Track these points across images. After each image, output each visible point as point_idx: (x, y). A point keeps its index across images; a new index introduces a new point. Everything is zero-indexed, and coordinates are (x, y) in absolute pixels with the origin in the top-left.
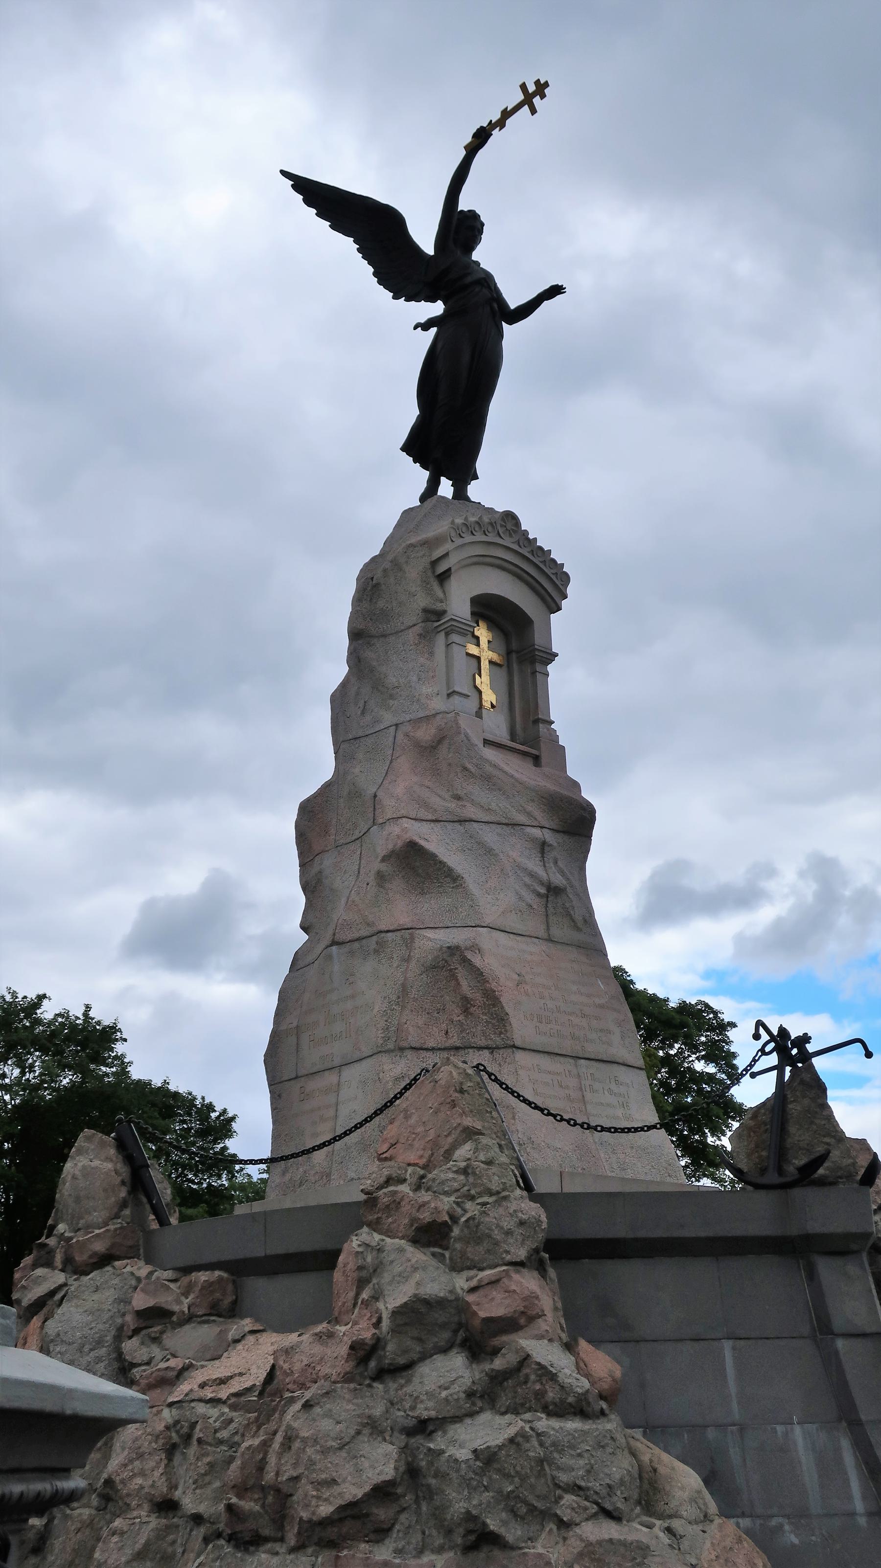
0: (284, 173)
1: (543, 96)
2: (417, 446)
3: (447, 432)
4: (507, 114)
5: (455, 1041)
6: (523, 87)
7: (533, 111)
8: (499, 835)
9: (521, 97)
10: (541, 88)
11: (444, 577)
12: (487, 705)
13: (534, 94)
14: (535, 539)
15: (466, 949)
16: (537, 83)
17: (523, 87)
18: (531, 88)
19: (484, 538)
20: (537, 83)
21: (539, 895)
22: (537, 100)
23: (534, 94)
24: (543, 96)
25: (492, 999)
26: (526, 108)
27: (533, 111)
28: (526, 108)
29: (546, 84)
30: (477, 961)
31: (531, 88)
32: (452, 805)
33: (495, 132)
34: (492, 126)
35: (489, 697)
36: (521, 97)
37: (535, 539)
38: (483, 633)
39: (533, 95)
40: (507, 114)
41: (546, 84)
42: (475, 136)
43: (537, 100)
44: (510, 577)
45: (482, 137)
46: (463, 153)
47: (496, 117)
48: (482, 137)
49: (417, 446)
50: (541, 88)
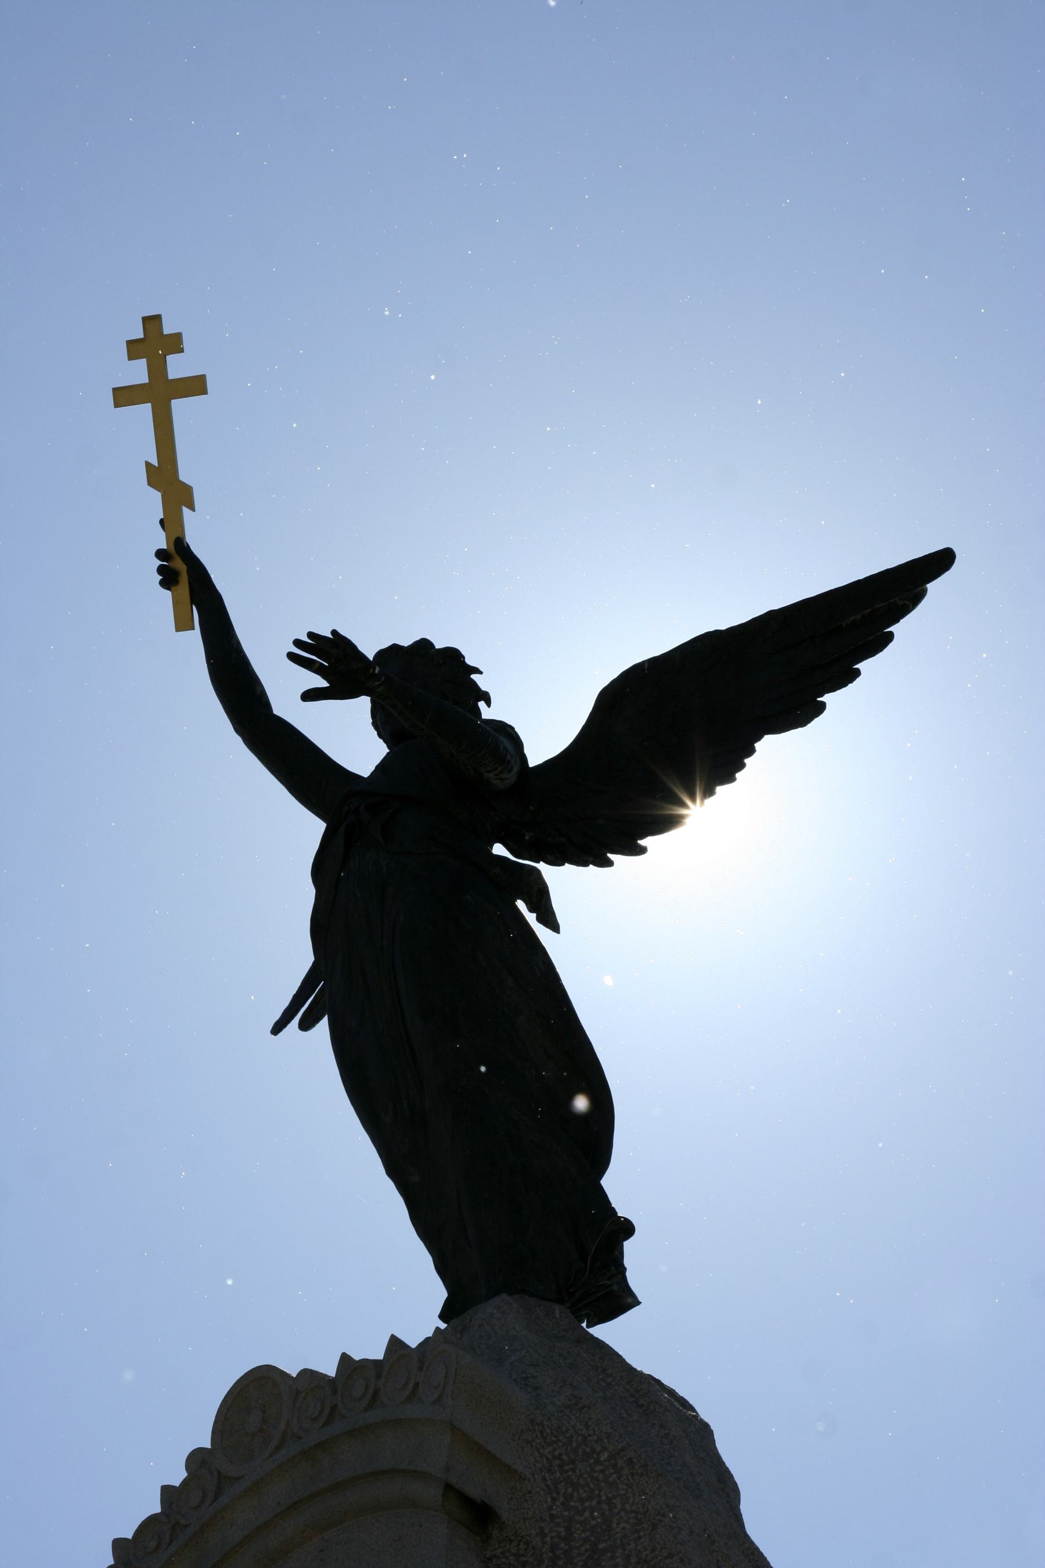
1: (175, 343)
6: (124, 396)
7: (196, 386)
9: (144, 412)
10: (154, 342)
13: (157, 369)
14: (395, 1343)
16: (134, 349)
17: (124, 396)
18: (138, 373)
20: (134, 349)
22: (177, 367)
23: (157, 369)
24: (175, 343)
26: (180, 407)
27: (196, 386)
28: (180, 407)
29: (152, 322)
31: (138, 373)
34: (171, 522)
36: (144, 412)
37: (395, 1343)
39: (159, 375)
41: (152, 322)
42: (168, 579)
43: (177, 367)
46: (194, 638)
47: (153, 502)
50: (154, 342)
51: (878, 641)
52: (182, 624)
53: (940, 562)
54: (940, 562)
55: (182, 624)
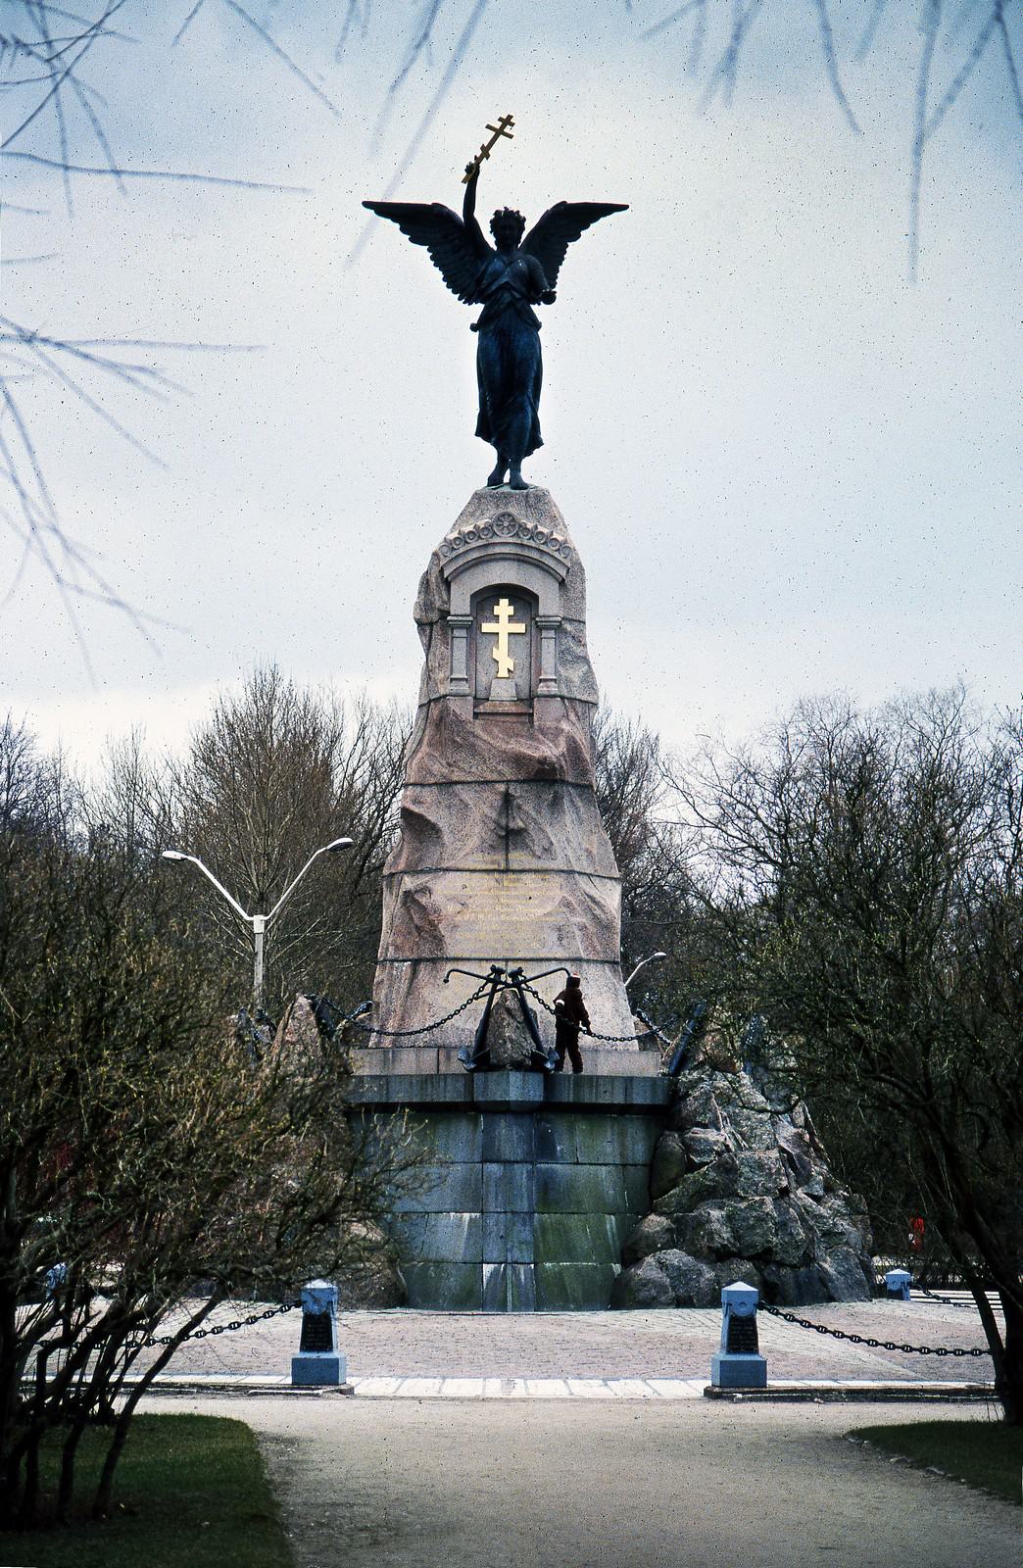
0: (367, 204)
1: (512, 125)
2: (484, 431)
3: (509, 407)
4: (485, 151)
5: (414, 956)
7: (511, 137)
8: (476, 791)
10: (507, 121)
11: (447, 584)
12: (503, 673)
13: (503, 127)
15: (416, 892)
16: (500, 119)
18: (498, 125)
19: (480, 543)
20: (500, 119)
21: (500, 837)
22: (507, 130)
25: (434, 926)
27: (511, 137)
28: (501, 137)
30: (423, 900)
31: (498, 125)
32: (445, 771)
33: (484, 164)
34: (478, 160)
35: (506, 663)
38: (504, 608)
40: (485, 151)
43: (507, 130)
44: (516, 564)
45: (472, 173)
47: (479, 153)
48: (472, 173)
49: (484, 431)
50: (507, 121)
51: (595, 220)
52: (464, 181)
53: (625, 207)
54: (625, 207)
55: (464, 181)
